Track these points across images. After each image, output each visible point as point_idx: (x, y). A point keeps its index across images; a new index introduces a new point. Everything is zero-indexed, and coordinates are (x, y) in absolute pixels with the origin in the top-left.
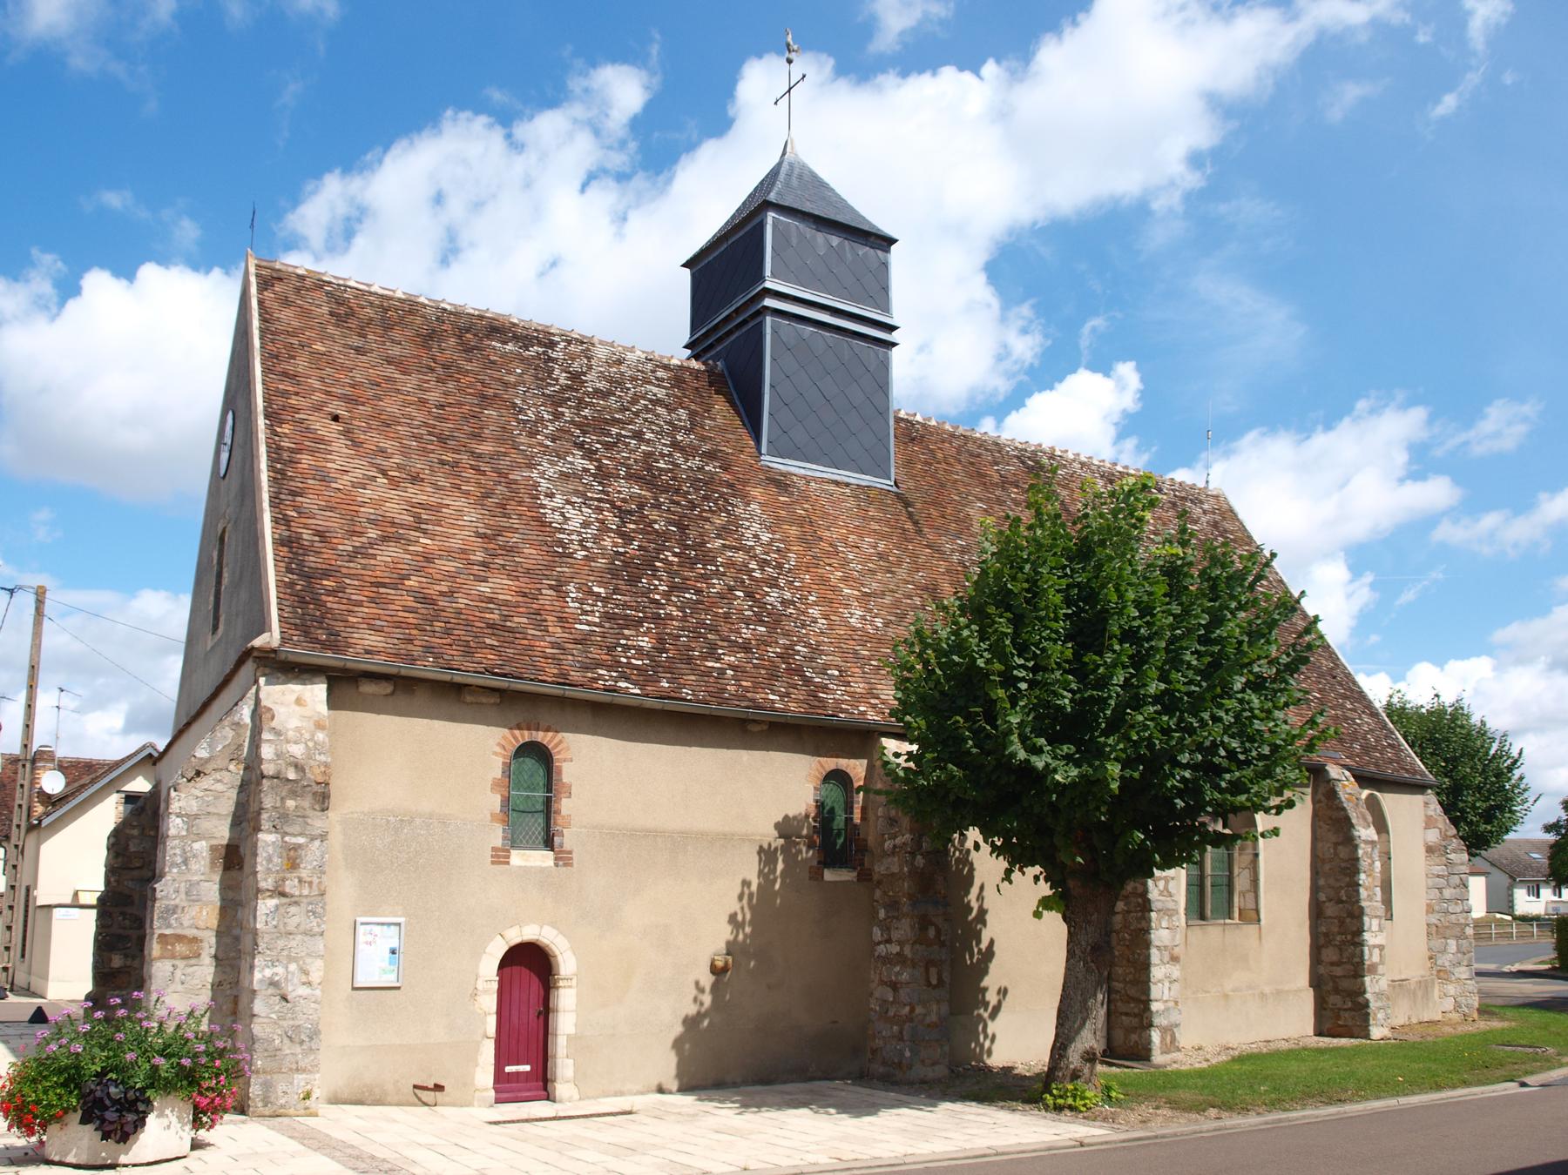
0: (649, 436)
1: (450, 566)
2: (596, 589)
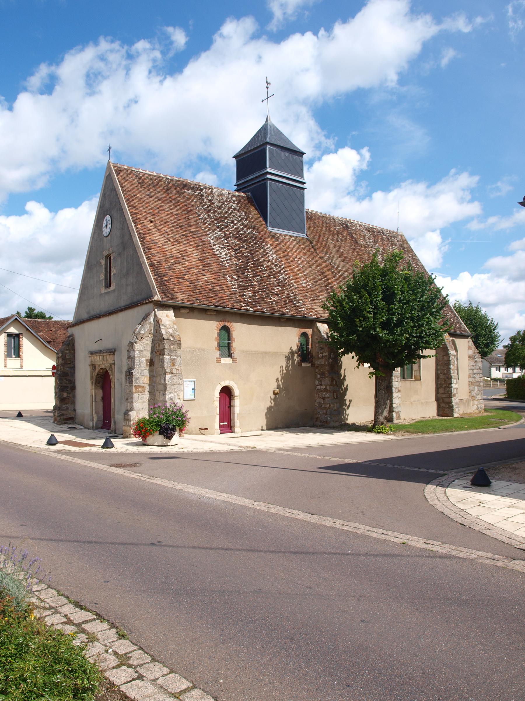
0: (236, 222)
1: (194, 271)
2: (234, 277)
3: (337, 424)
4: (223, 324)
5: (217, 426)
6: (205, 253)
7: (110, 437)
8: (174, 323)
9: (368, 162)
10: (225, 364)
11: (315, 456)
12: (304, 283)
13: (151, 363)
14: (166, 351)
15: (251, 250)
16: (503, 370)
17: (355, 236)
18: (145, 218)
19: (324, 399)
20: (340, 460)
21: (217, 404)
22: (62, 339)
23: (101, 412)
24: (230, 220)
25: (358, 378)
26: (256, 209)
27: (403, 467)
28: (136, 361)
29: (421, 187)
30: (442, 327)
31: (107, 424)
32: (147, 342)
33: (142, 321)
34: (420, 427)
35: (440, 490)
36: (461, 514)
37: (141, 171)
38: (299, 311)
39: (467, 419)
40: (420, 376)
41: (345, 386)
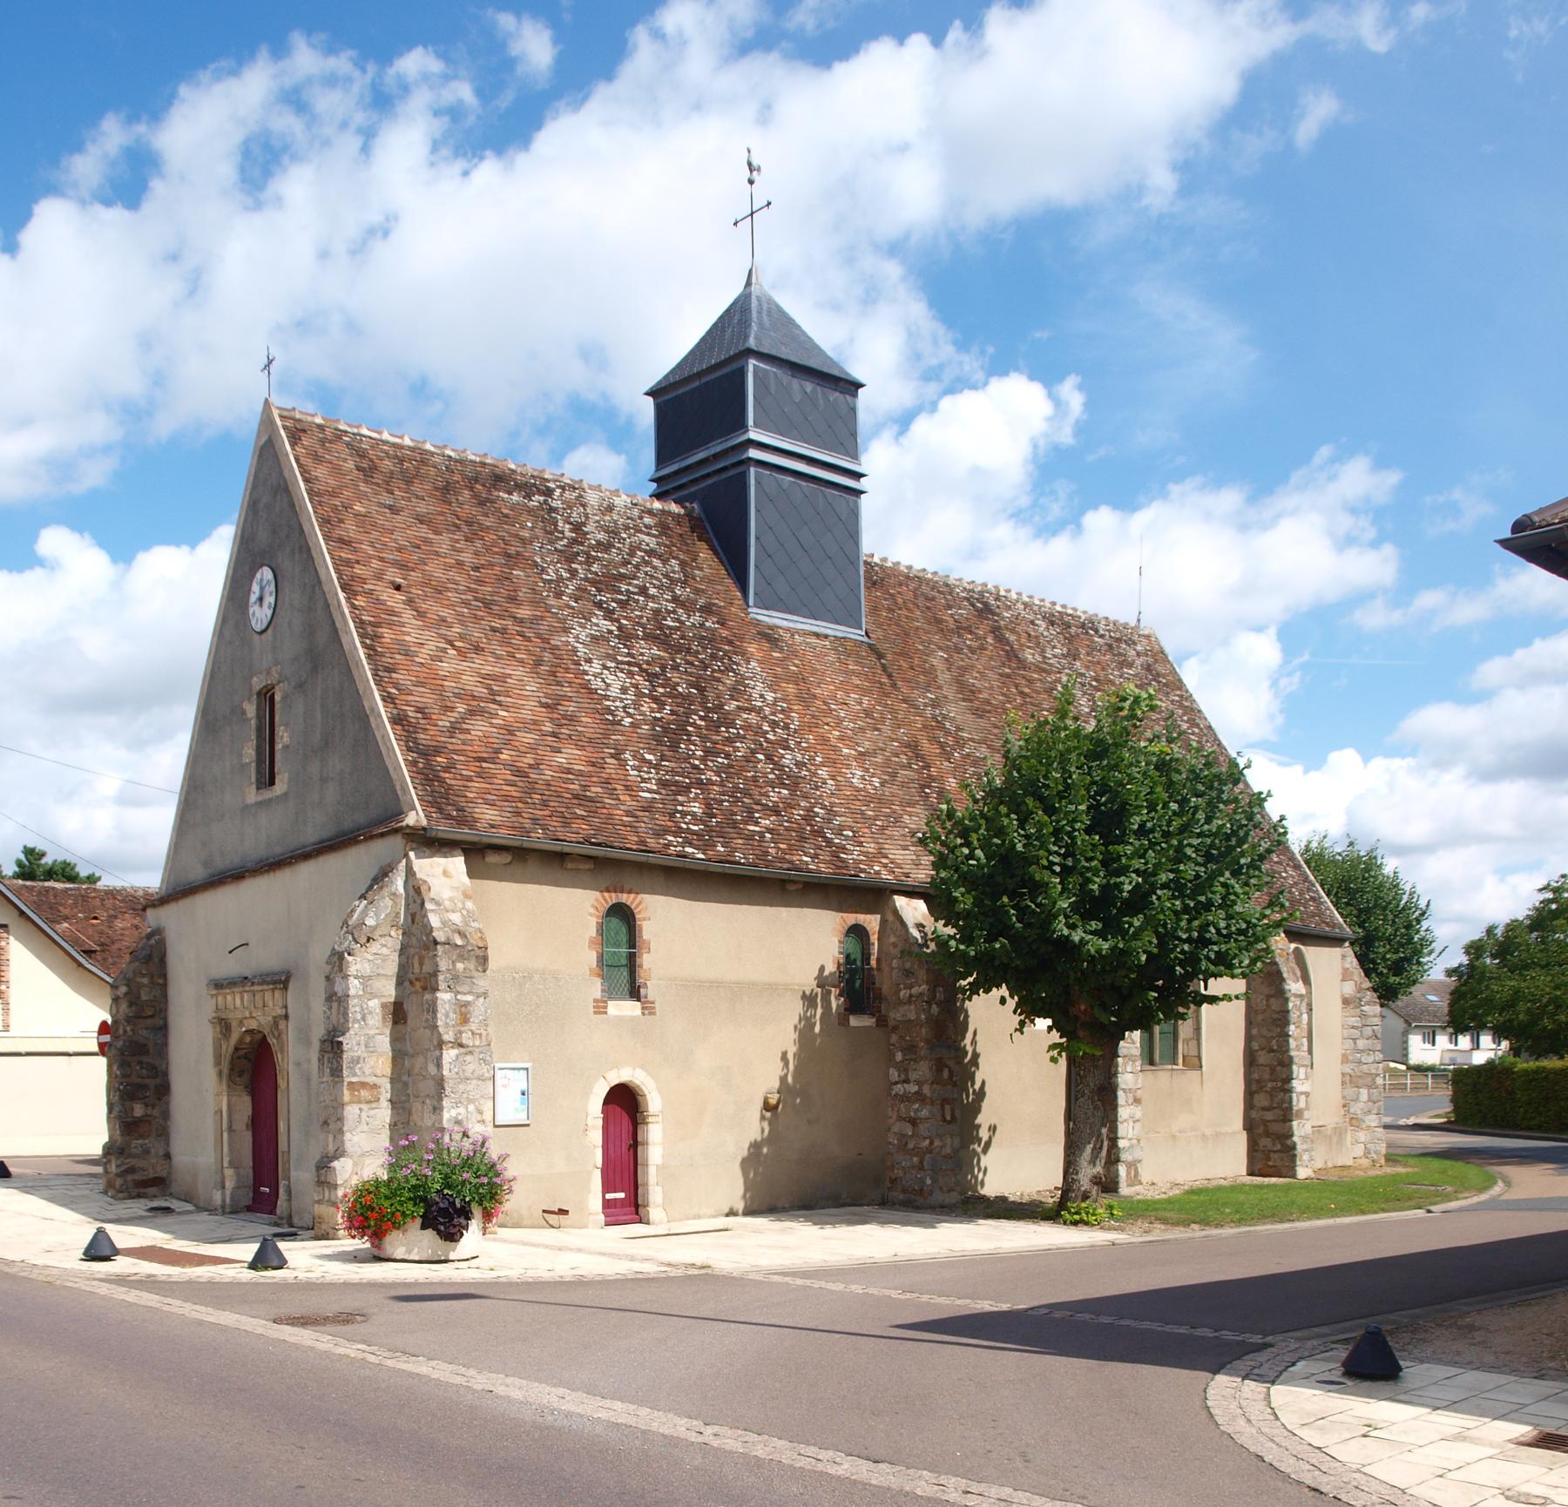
0: (652, 591)
1: (529, 738)
2: (648, 757)
3: (953, 1197)
4: (613, 898)
5: (595, 1203)
6: (559, 684)
7: (276, 1235)
8: (467, 896)
9: (1077, 422)
10: (620, 1019)
11: (887, 1292)
12: (856, 776)
13: (398, 1014)
14: (441, 978)
15: (699, 677)
16: (1442, 1040)
17: (1012, 638)
18: (379, 577)
20: (959, 1302)
21: (596, 1137)
22: (129, 941)
23: (248, 1161)
24: (636, 586)
25: (1014, 1059)
26: (716, 553)
27: (1146, 1325)
28: (352, 1010)
29: (1229, 499)
30: (1268, 912)
31: (265, 1196)
32: (385, 951)
33: (371, 887)
34: (1199, 1206)
35: (1252, 1388)
36: (1313, 1461)
37: (365, 431)
38: (843, 861)
39: (1335, 1184)
40: (1199, 1057)
41: (977, 1087)
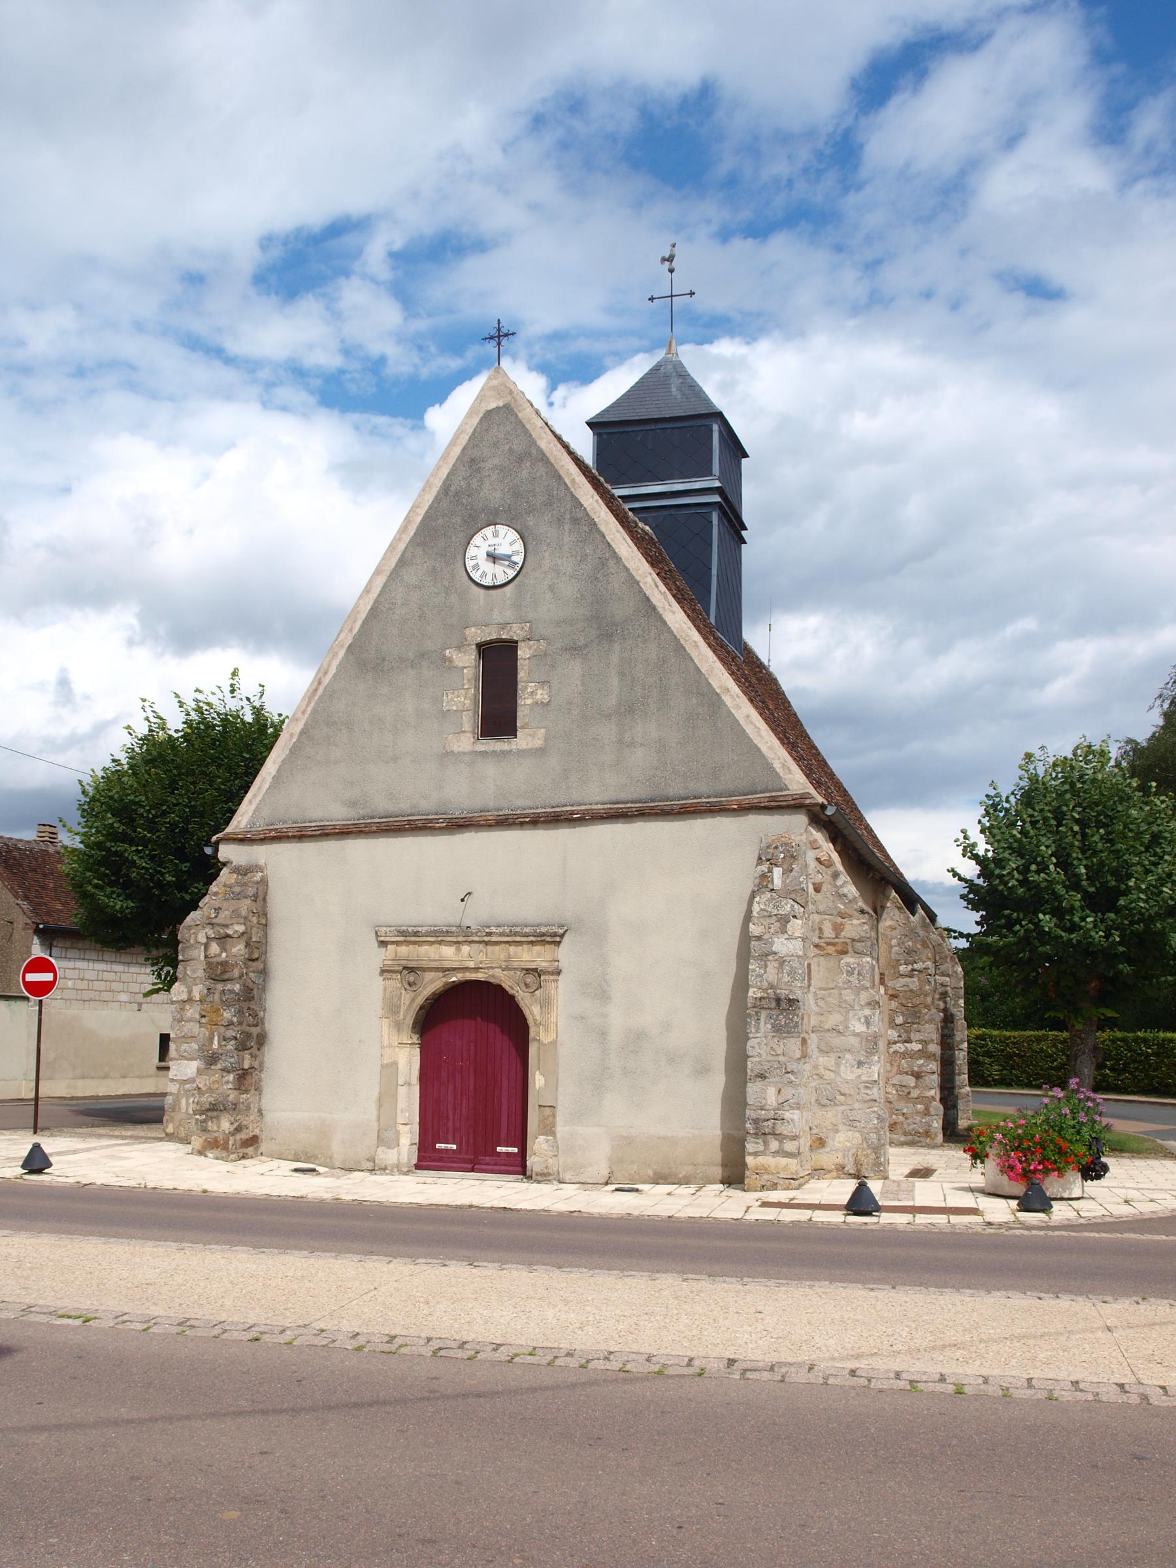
19: (918, 1076)
